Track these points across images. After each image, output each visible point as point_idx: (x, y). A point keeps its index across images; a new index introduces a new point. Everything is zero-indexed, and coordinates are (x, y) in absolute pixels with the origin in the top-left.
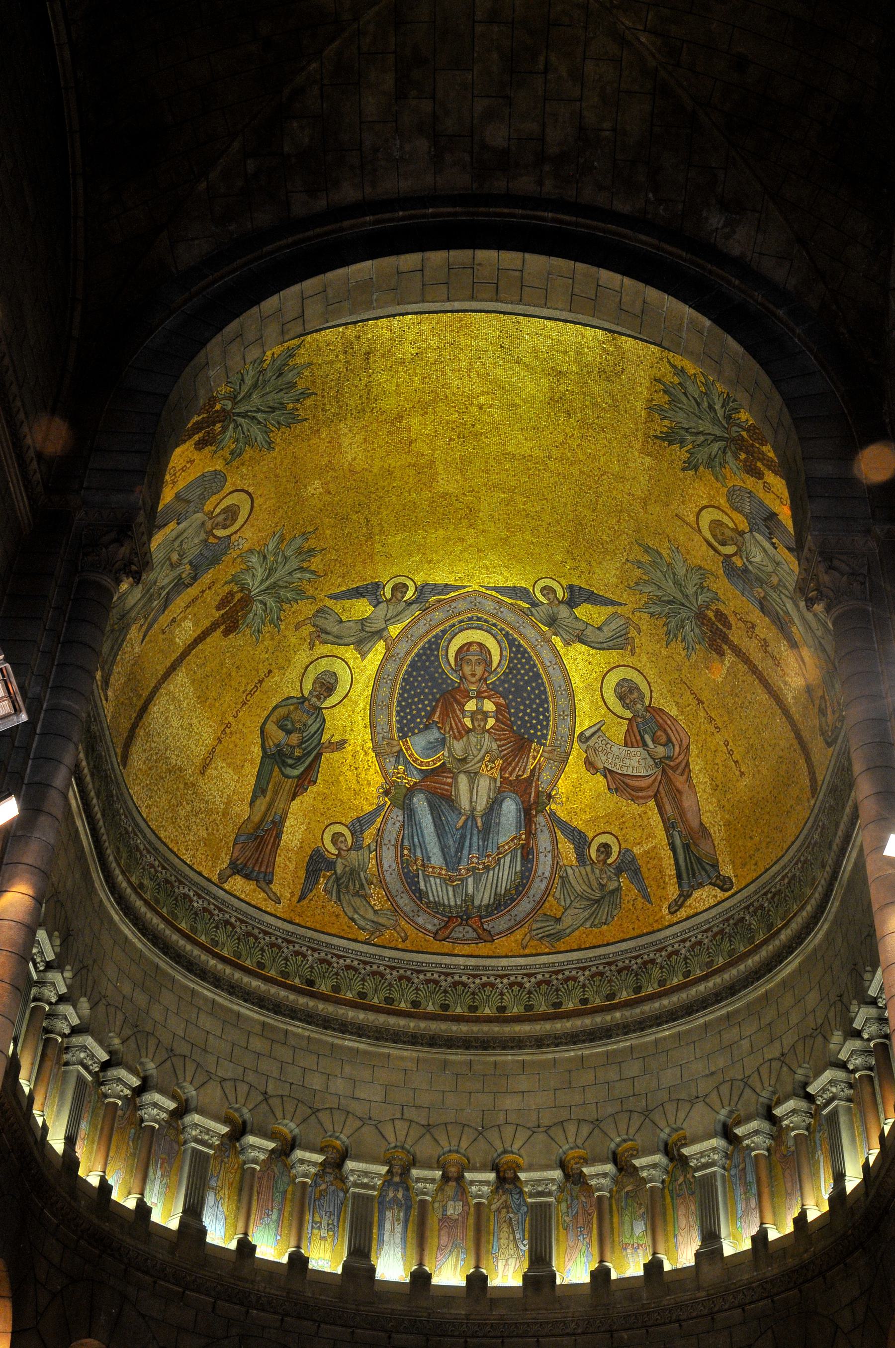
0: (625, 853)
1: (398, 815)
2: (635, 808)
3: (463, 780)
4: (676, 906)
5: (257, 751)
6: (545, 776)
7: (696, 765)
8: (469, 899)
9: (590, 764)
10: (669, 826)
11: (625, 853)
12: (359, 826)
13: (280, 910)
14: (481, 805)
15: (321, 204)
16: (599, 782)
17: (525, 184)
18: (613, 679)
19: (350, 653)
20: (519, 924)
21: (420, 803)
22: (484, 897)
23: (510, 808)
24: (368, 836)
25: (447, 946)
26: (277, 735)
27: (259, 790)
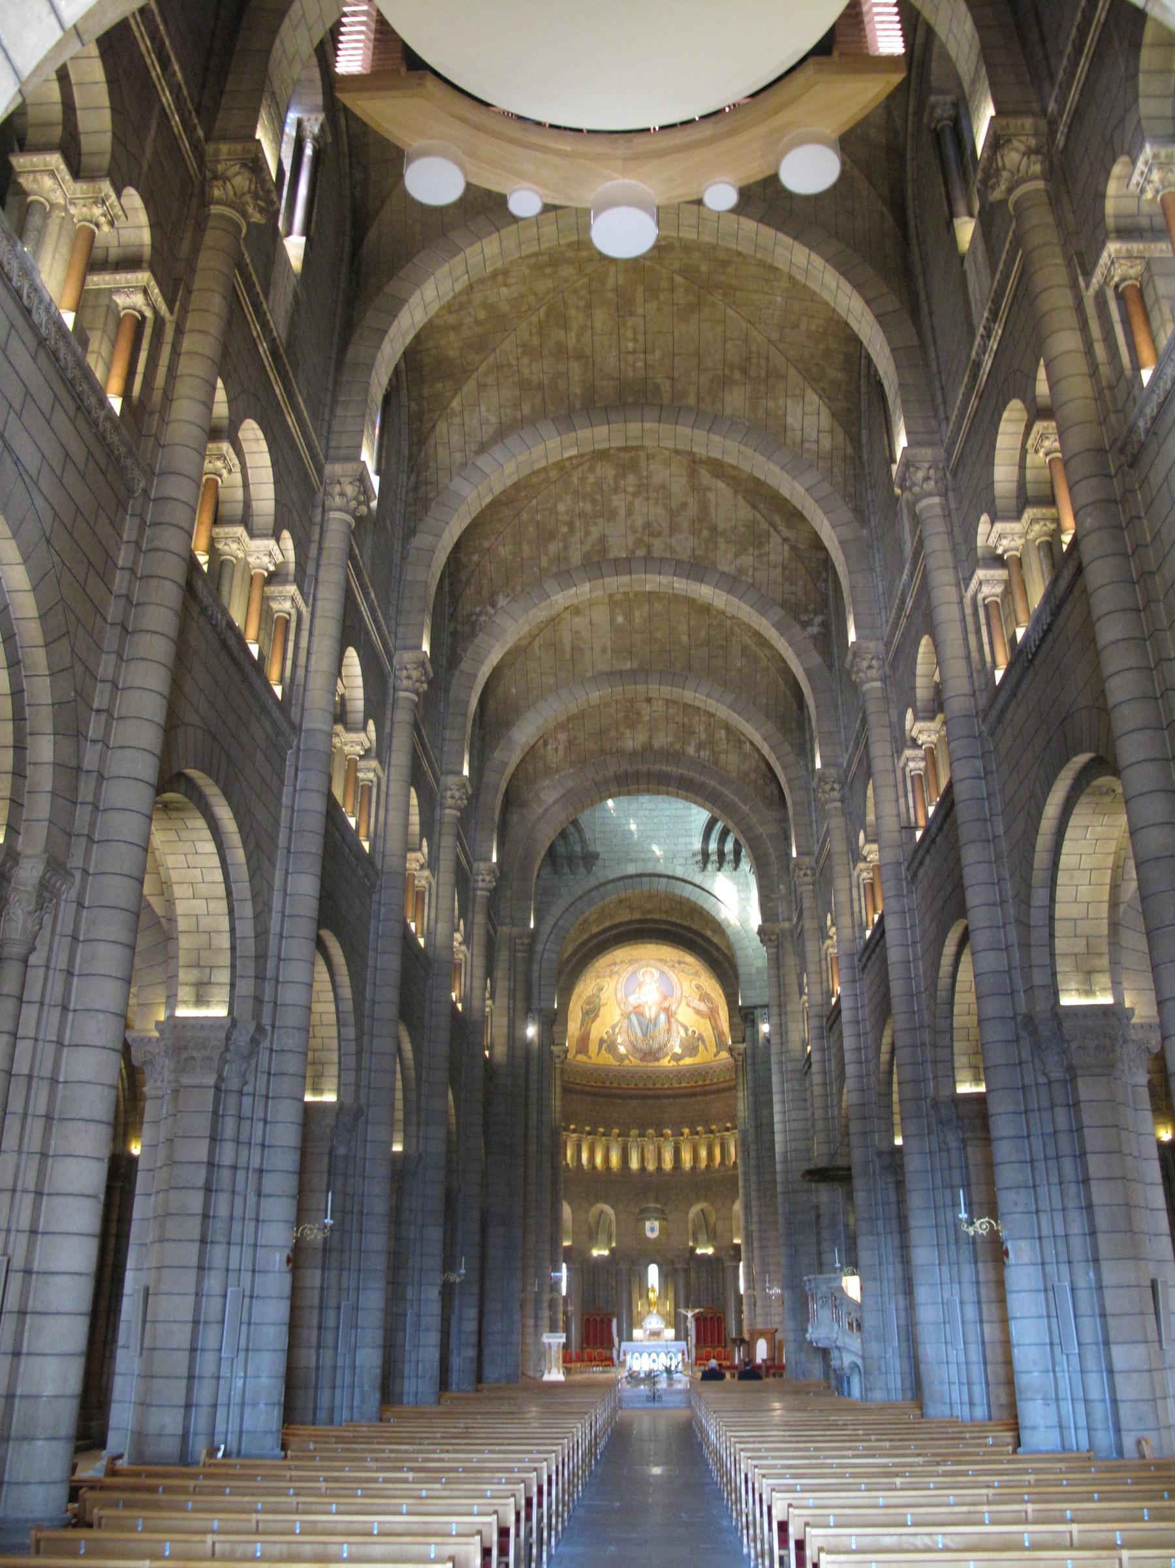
0: (700, 1035)
1: (626, 1021)
2: (702, 1020)
3: (647, 1009)
4: (716, 1055)
5: (580, 1014)
6: (674, 1008)
7: (721, 1012)
8: (651, 1048)
9: (688, 1005)
10: (713, 1029)
11: (700, 1035)
12: (613, 1028)
13: (593, 1061)
14: (653, 1016)
15: (600, 928)
16: (691, 1011)
17: (656, 916)
18: (694, 983)
19: (608, 979)
20: (667, 1055)
21: (633, 1018)
22: (656, 1046)
23: (663, 1017)
24: (617, 1030)
25: (644, 1064)
26: (586, 1007)
27: (582, 1024)
